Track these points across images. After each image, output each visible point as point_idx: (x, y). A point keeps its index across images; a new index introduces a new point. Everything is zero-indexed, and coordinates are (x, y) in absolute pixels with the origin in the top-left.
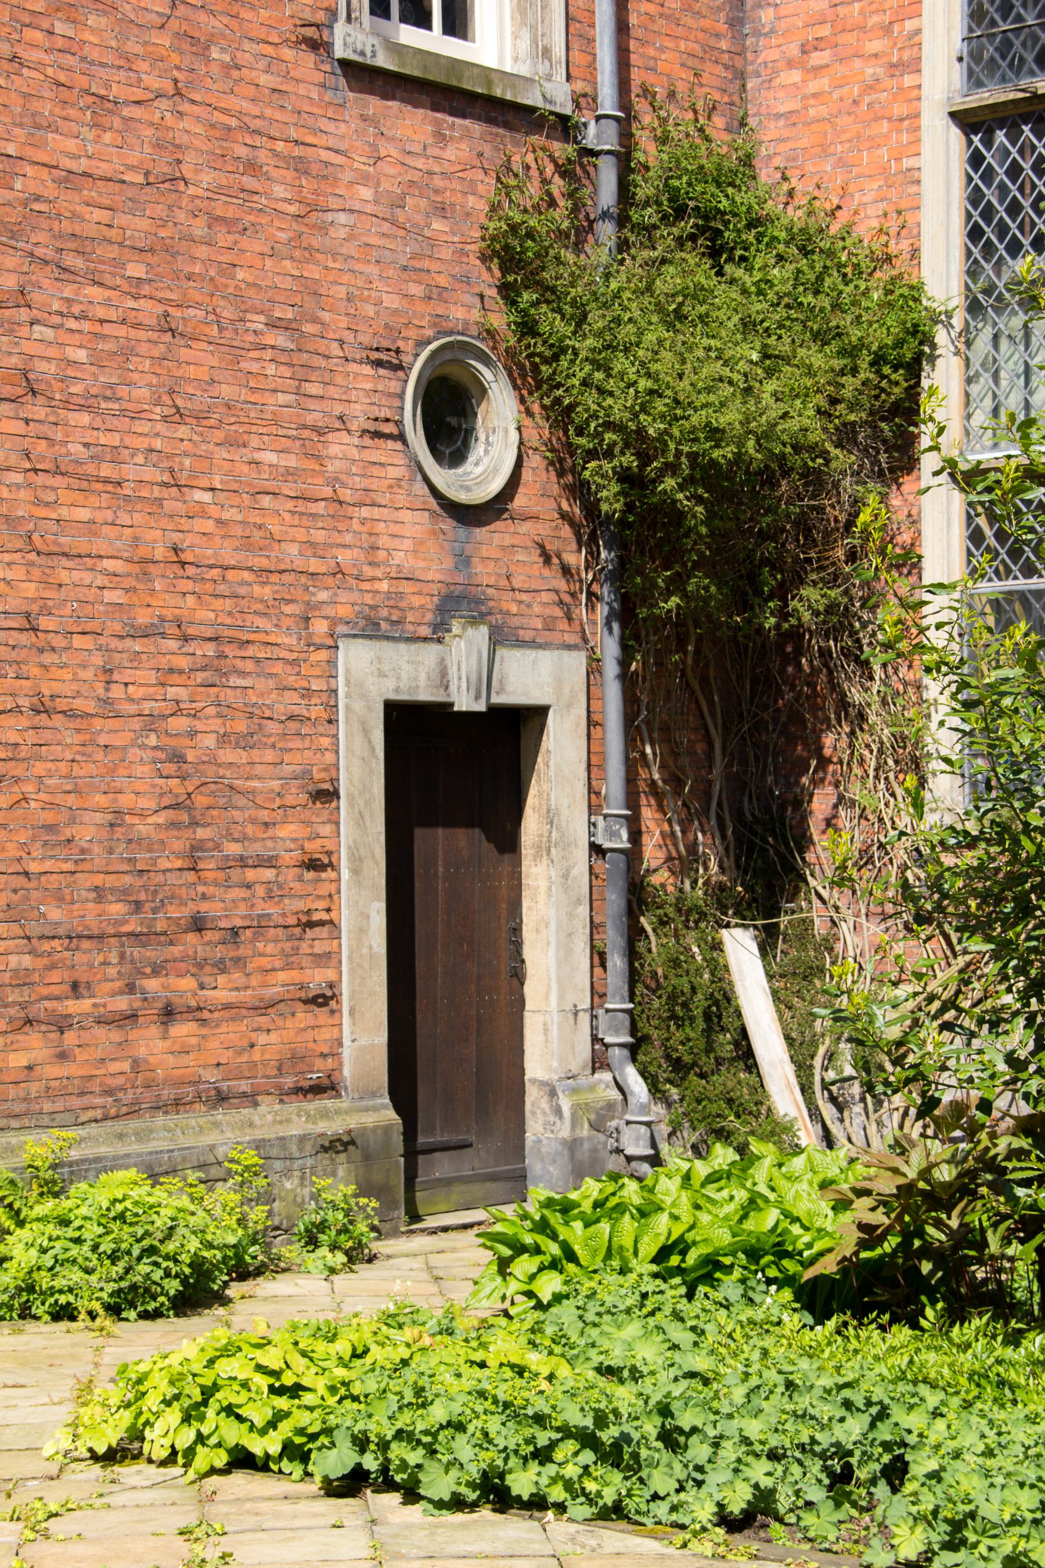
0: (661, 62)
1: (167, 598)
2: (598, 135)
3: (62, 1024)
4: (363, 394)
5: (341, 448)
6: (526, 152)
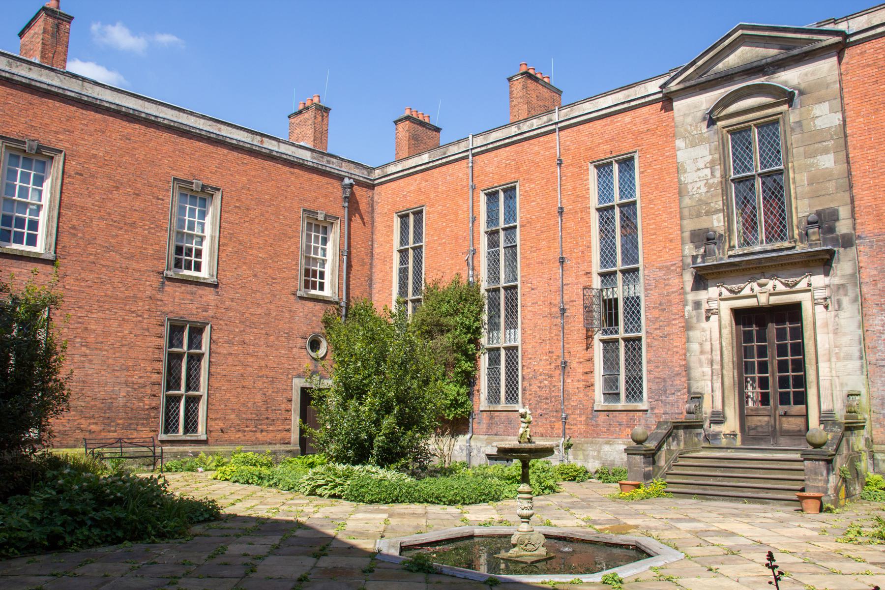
0: (355, 293)
1: (264, 372)
2: (343, 304)
3: (245, 431)
4: (300, 342)
5: (295, 350)
6: (330, 307)
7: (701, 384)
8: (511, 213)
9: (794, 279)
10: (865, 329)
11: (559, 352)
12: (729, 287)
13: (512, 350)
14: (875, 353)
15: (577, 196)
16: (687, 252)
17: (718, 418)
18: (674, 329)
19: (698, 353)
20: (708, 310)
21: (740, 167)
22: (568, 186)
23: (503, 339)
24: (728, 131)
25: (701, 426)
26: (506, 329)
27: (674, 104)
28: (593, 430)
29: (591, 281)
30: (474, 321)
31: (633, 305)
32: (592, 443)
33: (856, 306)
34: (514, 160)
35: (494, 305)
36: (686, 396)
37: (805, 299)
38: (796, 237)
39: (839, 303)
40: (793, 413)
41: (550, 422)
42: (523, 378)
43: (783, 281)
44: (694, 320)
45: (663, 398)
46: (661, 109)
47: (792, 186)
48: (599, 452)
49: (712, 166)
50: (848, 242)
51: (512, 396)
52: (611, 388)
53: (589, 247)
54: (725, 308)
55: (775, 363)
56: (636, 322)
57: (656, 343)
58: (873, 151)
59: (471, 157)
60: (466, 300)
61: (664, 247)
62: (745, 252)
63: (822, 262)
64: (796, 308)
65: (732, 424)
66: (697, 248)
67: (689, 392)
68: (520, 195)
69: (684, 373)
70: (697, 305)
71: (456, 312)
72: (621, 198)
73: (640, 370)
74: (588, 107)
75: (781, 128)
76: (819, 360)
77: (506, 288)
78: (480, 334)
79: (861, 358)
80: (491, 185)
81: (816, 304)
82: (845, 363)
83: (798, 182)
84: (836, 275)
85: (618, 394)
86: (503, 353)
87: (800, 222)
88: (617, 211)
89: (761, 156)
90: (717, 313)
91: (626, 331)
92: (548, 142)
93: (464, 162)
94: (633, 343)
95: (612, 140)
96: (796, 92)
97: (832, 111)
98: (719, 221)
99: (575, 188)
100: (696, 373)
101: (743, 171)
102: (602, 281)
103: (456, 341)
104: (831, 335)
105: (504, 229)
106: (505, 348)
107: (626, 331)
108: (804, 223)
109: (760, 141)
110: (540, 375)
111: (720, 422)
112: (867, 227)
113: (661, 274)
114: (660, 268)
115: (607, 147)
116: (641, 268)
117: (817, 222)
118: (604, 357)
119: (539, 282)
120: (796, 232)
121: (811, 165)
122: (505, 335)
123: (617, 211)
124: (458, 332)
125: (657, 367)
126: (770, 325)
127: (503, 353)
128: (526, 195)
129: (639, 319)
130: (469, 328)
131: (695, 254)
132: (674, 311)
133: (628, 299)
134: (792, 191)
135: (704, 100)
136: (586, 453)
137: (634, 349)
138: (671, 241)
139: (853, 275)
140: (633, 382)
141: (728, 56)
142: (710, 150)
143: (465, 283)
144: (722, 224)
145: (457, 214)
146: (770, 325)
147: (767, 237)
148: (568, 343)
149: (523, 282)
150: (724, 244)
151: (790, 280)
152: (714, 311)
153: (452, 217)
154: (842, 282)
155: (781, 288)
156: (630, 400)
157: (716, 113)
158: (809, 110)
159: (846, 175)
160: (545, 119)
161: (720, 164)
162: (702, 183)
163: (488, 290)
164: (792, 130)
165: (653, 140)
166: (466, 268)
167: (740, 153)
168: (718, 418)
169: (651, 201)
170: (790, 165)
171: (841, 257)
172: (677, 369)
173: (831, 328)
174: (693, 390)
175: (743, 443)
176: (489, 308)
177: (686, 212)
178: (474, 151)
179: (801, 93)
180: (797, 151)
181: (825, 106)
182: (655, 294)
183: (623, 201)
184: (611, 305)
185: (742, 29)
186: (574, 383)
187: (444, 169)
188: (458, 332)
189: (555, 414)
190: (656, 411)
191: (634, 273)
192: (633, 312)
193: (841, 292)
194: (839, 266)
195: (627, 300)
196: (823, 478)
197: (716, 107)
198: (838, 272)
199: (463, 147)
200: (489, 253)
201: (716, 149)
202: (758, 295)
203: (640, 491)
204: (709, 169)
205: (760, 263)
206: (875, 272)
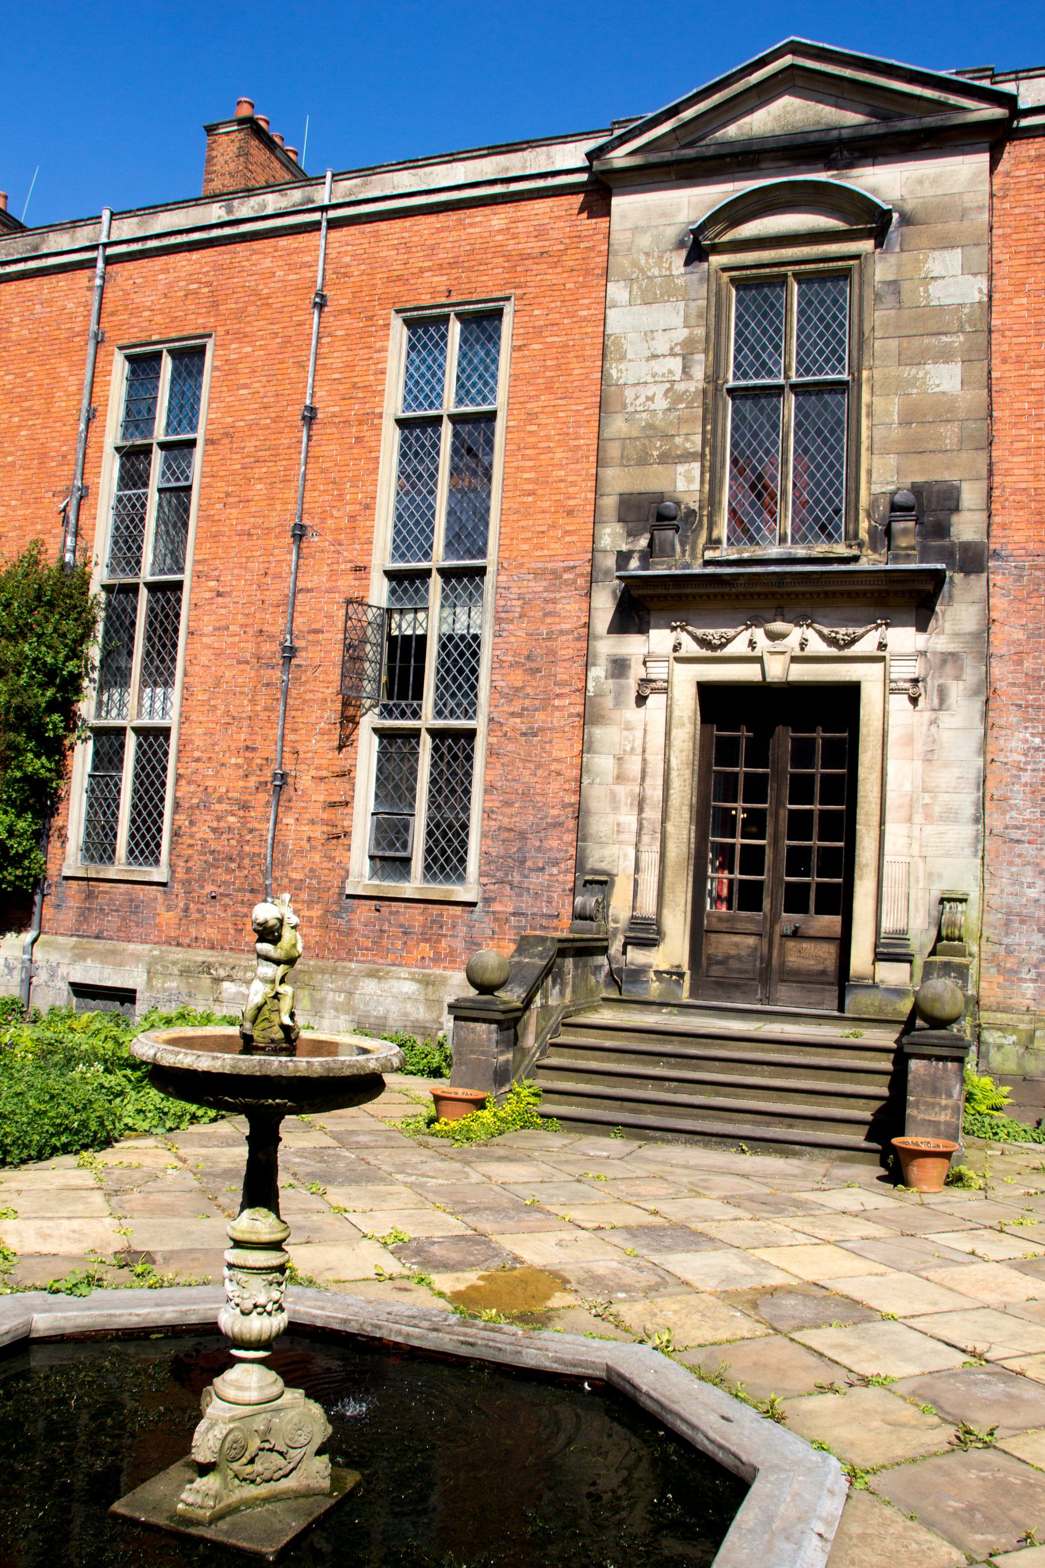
8: (184, 408)
9: (850, 630)
10: (989, 757)
11: (271, 750)
12: (699, 632)
13: (154, 737)
14: (1004, 813)
15: (354, 386)
17: (645, 934)
18: (557, 719)
19: (610, 779)
20: (645, 681)
21: (751, 365)
22: (336, 360)
23: (135, 707)
24: (732, 280)
25: (604, 950)
26: (144, 684)
27: (615, 201)
28: (340, 942)
29: (367, 588)
30: (68, 658)
31: (462, 654)
32: (334, 971)
33: (978, 705)
34: (209, 284)
35: (120, 625)
36: (570, 877)
37: (869, 678)
38: (863, 535)
39: (942, 693)
40: (812, 932)
41: (235, 915)
42: (177, 806)
43: (826, 631)
44: (609, 702)
45: (517, 878)
46: (581, 211)
48: (350, 994)
50: (973, 560)
51: (145, 847)
52: (391, 845)
53: (369, 507)
54: (684, 682)
55: (783, 815)
56: (466, 695)
57: (511, 747)
59: (100, 264)
60: (51, 605)
61: (553, 526)
62: (746, 555)
63: (914, 598)
64: (849, 694)
65: (674, 950)
67: (580, 865)
68: (215, 368)
69: (571, 824)
70: (619, 666)
71: (22, 633)
72: (460, 401)
73: (466, 809)
74: (405, 181)
75: (851, 291)
76: (889, 817)
77: (152, 587)
78: (78, 690)
79: (977, 820)
80: (143, 337)
81: (893, 691)
82: (942, 828)
83: (880, 412)
84: (942, 632)
85: (407, 861)
86: (131, 741)
87: (874, 503)
88: (447, 430)
89: (801, 345)
90: (665, 691)
91: (439, 714)
92: (297, 251)
93: (82, 277)
94: (455, 745)
95: (454, 264)
96: (895, 216)
97: (967, 269)
98: (690, 480)
99: (350, 366)
100: (600, 824)
101: (757, 375)
102: (393, 592)
103: (15, 702)
104: (918, 765)
105: (163, 446)
106: (137, 730)
107: (439, 714)
108: (883, 507)
109: (801, 312)
110: (220, 801)
111: (649, 943)
112: (1015, 535)
113: (538, 586)
114: (538, 574)
115: (440, 281)
117: (910, 509)
118: (380, 769)
119: (239, 577)
120: (864, 525)
121: (912, 382)
122: (140, 698)
123: (447, 430)
124: (23, 680)
125: (508, 804)
126: (780, 729)
127: (131, 741)
128: (228, 370)
129: (473, 687)
130: (51, 673)
131: (624, 548)
132: (562, 677)
133: (450, 638)
135: (685, 201)
136: (318, 995)
137: (455, 757)
138: (570, 513)
139: (976, 636)
140: (444, 834)
141: (752, 111)
142: (686, 317)
143: (53, 564)
144: (696, 486)
145: (49, 398)
146: (780, 729)
147: (795, 530)
148: (294, 731)
149: (198, 575)
150: (696, 532)
151: (843, 631)
152: (660, 684)
153: (37, 404)
154: (952, 648)
155: (817, 646)
156: (434, 877)
157: (711, 233)
158: (917, 261)
159: (984, 413)
160: (296, 196)
161: (706, 351)
162: (660, 390)
163: (107, 588)
164: (878, 297)
165: (553, 277)
166: (59, 530)
167: (754, 332)
168: (645, 934)
170: (865, 374)
171: (956, 592)
172: (554, 812)
173: (919, 747)
174: (592, 863)
175: (693, 994)
176: (107, 632)
177: (613, 450)
178: (110, 251)
179: (906, 220)
180: (882, 346)
181: (954, 258)
182: (518, 633)
183: (463, 409)
184: (406, 653)
185: (794, 53)
186: (298, 828)
187: (29, 286)
188: (23, 680)
190: (496, 907)
191: (471, 579)
192: (461, 671)
193: (949, 669)
194: (950, 612)
195: (447, 642)
196: (950, 1102)
197: (714, 219)
198: (947, 625)
199: (84, 236)
200: (120, 500)
201: (699, 316)
202: (767, 658)
203: (486, 1115)
204: (679, 359)
205: (780, 584)
206: (1019, 635)
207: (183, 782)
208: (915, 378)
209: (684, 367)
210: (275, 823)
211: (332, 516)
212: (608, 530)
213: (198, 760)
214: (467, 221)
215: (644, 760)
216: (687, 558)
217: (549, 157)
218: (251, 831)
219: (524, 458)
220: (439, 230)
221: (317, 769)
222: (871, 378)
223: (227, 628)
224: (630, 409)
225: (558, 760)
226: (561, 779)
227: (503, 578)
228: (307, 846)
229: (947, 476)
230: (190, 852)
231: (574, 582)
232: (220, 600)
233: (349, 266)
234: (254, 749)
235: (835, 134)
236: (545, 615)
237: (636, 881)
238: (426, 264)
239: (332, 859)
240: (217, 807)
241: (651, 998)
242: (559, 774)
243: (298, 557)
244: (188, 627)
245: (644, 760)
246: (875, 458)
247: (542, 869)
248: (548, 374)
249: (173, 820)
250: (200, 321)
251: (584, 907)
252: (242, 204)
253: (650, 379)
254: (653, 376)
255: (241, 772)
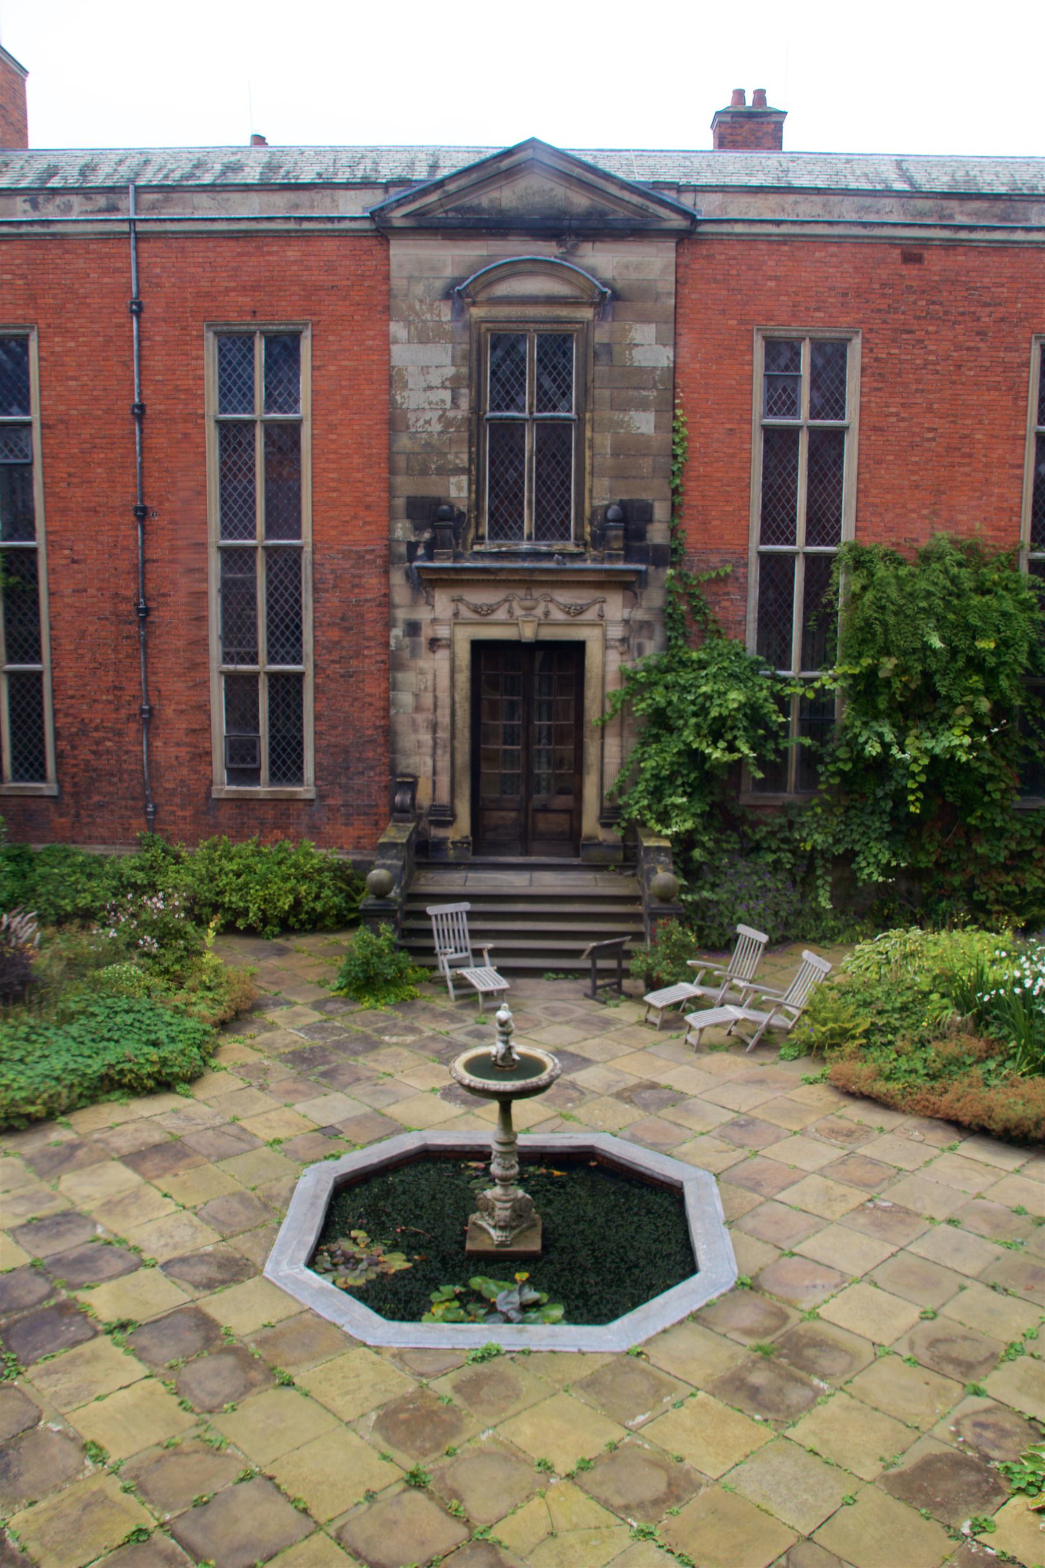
7: (414, 760)
15: (177, 389)
16: (399, 534)
17: (444, 816)
19: (410, 710)
21: (503, 399)
24: (488, 330)
40: (554, 807)
42: (57, 735)
44: (406, 654)
45: (344, 781)
47: (588, 453)
49: (454, 385)
52: (243, 760)
57: (333, 686)
58: (708, 421)
61: (355, 517)
65: (462, 826)
66: (418, 529)
69: (382, 740)
70: (413, 628)
84: (640, 606)
85: (258, 770)
87: (594, 513)
95: (255, 288)
97: (660, 341)
101: (508, 408)
107: (272, 660)
110: (96, 729)
113: (347, 564)
114: (346, 555)
116: (308, 549)
120: (588, 529)
121: (620, 424)
125: (334, 727)
131: (413, 539)
132: (369, 633)
134: (588, 461)
138: (368, 507)
142: (453, 357)
144: (464, 494)
147: (538, 528)
149: (49, 543)
154: (646, 617)
155: (558, 615)
161: (469, 387)
168: (444, 816)
169: (332, 428)
170: (588, 415)
172: (369, 732)
177: (401, 462)
179: (616, 296)
180: (602, 394)
182: (333, 600)
186: (169, 750)
189: (130, 803)
190: (330, 802)
193: (645, 632)
198: (644, 603)
201: (464, 358)
204: (449, 393)
207: (61, 715)
208: (623, 421)
209: (453, 399)
210: (149, 745)
211: (168, 500)
212: (400, 525)
213: (72, 697)
214: (265, 249)
215: (435, 697)
216: (460, 549)
217: (333, 201)
218: (127, 752)
219: (328, 461)
220: (241, 255)
221: (178, 703)
222: (592, 419)
223: (86, 591)
224: (413, 430)
225: (370, 695)
226: (372, 708)
227: (318, 557)
228: (176, 763)
229: (644, 496)
230: (75, 770)
231: (374, 561)
232: (76, 566)
233: (159, 276)
234: (121, 689)
235: (566, 223)
236: (353, 587)
237: (434, 783)
238: (232, 284)
239: (197, 772)
240: (95, 734)
241: (450, 860)
242: (371, 705)
243: (143, 533)
244: (49, 589)
245: (435, 697)
246: (595, 480)
247: (362, 773)
248: (344, 392)
249: (56, 747)
250: (20, 312)
251: (402, 802)
252: (48, 201)
253: (427, 406)
254: (430, 403)
255: (113, 707)
